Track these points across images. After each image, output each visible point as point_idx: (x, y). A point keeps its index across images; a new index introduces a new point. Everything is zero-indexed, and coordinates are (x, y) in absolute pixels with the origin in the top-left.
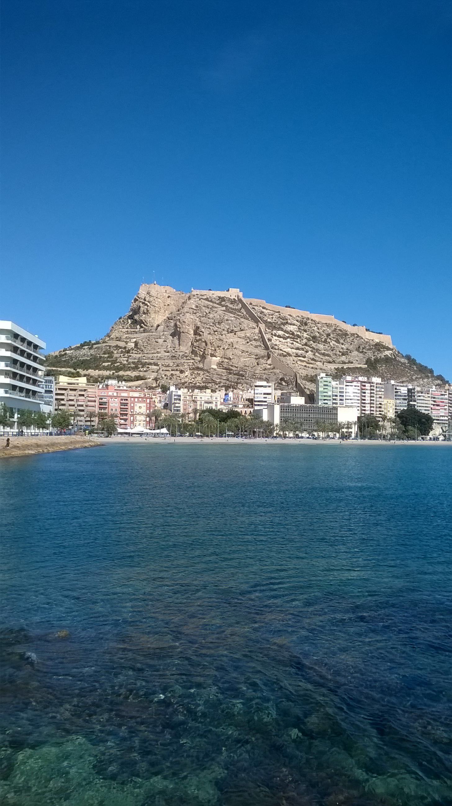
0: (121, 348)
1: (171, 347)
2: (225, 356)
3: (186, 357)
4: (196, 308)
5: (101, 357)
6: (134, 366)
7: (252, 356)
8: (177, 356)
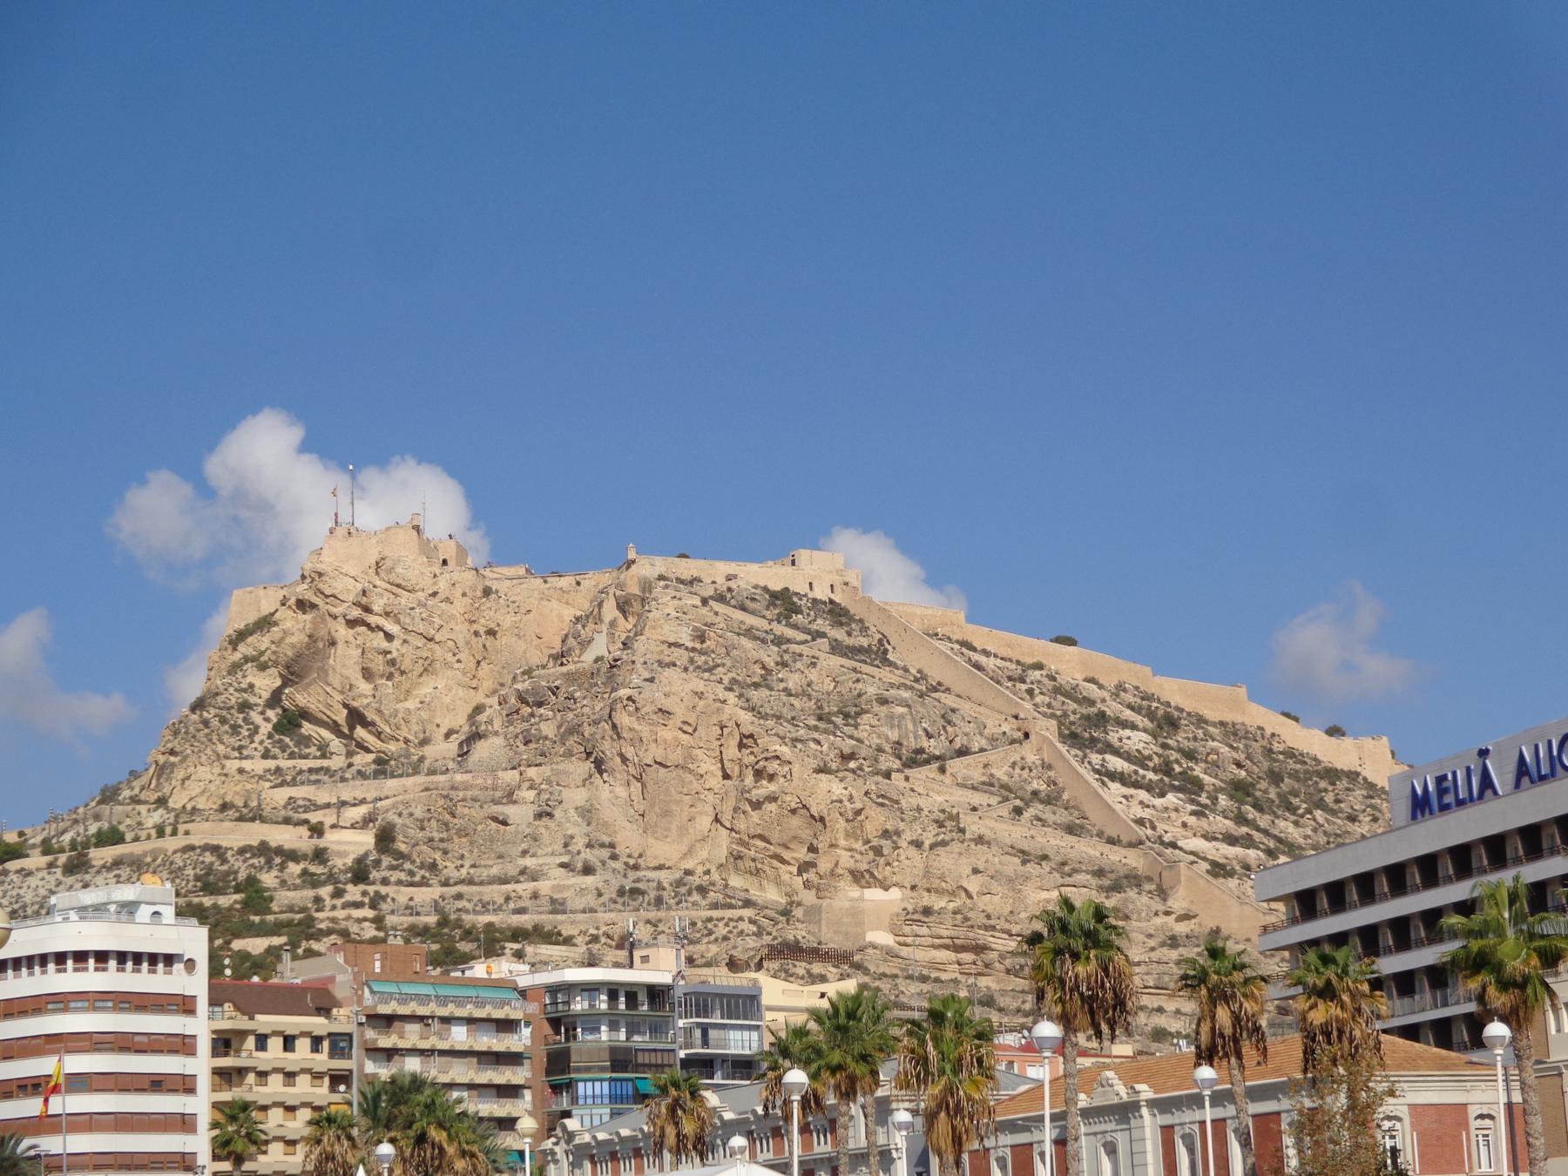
2: (936, 883)
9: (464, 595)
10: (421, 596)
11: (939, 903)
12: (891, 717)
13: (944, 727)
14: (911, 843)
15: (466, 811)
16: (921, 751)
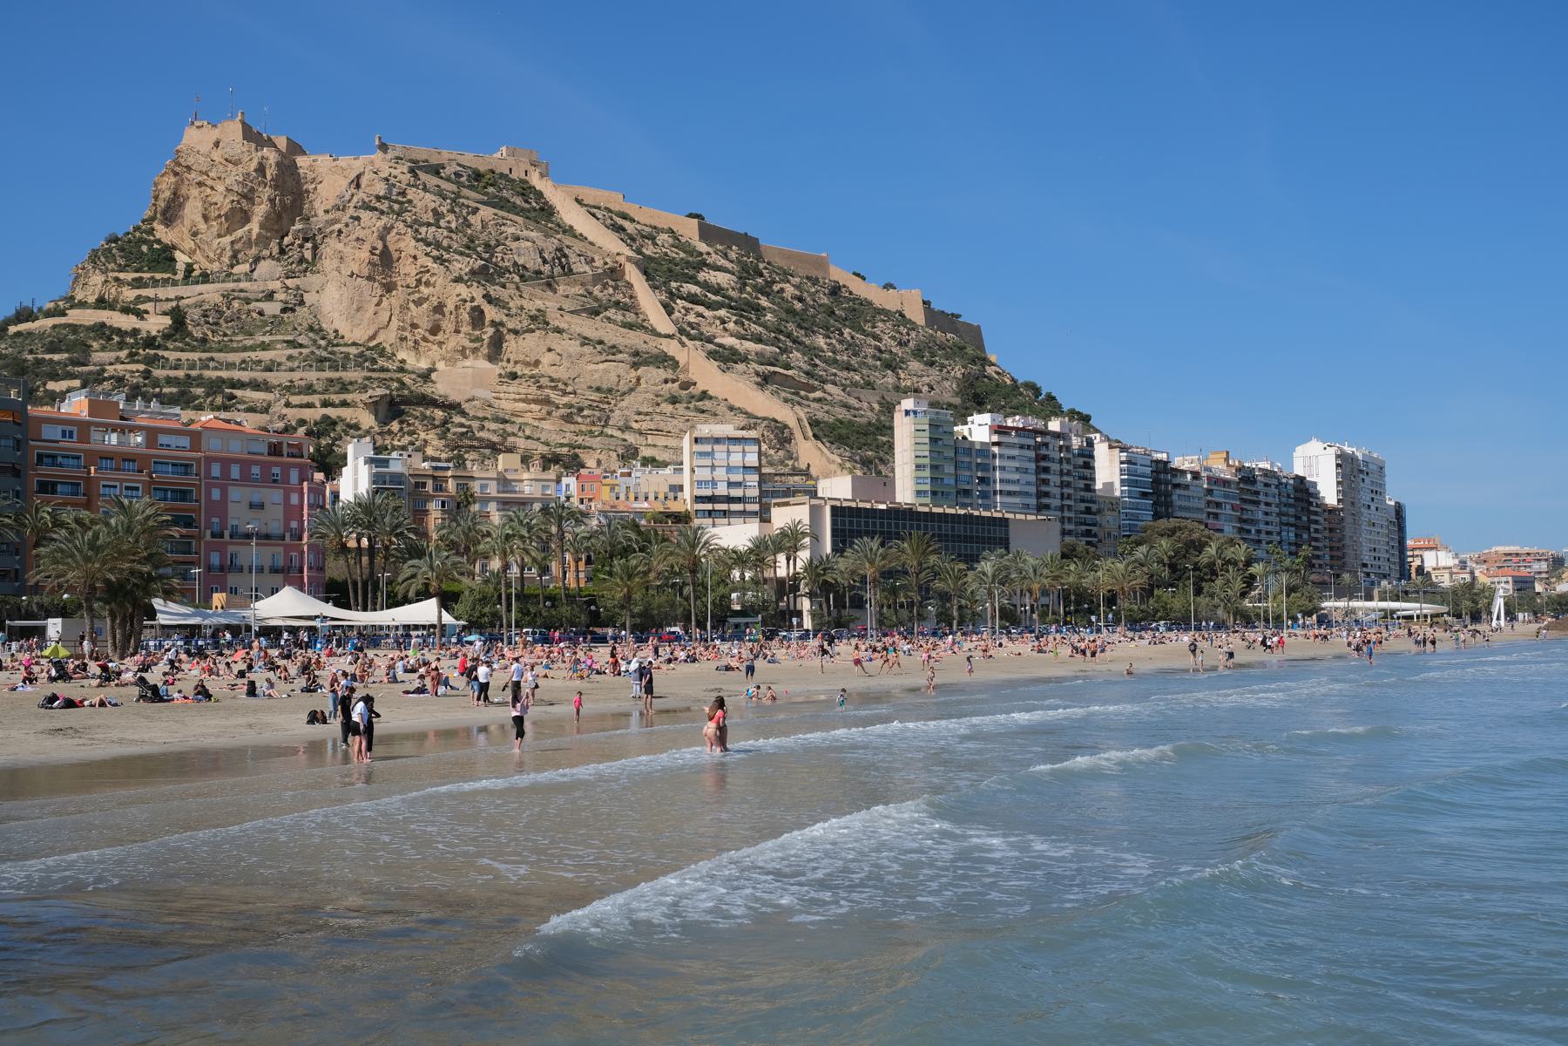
0: (119, 331)
2: (522, 357)
6: (174, 390)
7: (620, 356)
11: (519, 369)
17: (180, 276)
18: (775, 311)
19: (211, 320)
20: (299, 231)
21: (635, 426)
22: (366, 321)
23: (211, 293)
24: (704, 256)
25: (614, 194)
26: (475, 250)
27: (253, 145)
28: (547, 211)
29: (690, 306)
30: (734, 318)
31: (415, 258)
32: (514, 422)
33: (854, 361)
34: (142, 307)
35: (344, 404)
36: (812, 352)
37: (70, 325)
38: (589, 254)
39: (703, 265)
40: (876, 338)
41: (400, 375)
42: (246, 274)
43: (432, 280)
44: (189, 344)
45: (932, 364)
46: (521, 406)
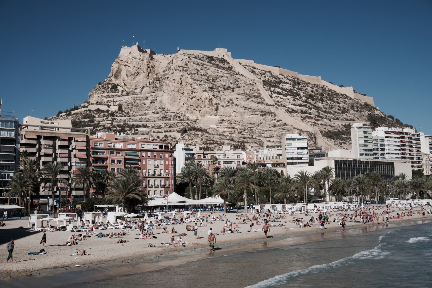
0: (103, 111)
1: (160, 108)
2: (225, 114)
3: (179, 117)
4: (186, 66)
5: (81, 122)
6: (120, 129)
7: (257, 113)
8: (169, 117)
9: (146, 59)
10: (137, 59)
11: (225, 118)
12: (223, 80)
13: (235, 82)
14: (222, 106)
15: (137, 102)
16: (230, 87)
17: (120, 94)
18: (305, 96)
19: (130, 107)
20: (155, 78)
21: (263, 135)
22: (176, 105)
23: (129, 98)
24: (281, 79)
25: (251, 61)
26: (209, 81)
27: (141, 53)
28: (230, 68)
29: (278, 95)
30: (293, 99)
31: (191, 84)
32: (223, 135)
33: (332, 111)
34: (109, 104)
35: (171, 131)
36: (318, 108)
37: (89, 110)
38: (245, 80)
39: (281, 82)
40: (338, 103)
41: (187, 121)
42: (140, 92)
43: (197, 91)
44: (123, 114)
45: (357, 111)
46: (226, 130)
